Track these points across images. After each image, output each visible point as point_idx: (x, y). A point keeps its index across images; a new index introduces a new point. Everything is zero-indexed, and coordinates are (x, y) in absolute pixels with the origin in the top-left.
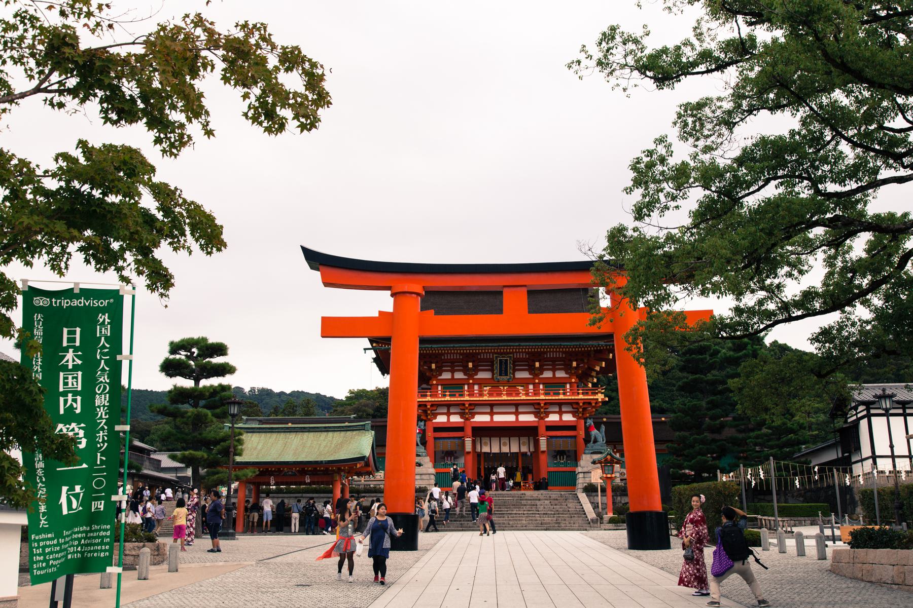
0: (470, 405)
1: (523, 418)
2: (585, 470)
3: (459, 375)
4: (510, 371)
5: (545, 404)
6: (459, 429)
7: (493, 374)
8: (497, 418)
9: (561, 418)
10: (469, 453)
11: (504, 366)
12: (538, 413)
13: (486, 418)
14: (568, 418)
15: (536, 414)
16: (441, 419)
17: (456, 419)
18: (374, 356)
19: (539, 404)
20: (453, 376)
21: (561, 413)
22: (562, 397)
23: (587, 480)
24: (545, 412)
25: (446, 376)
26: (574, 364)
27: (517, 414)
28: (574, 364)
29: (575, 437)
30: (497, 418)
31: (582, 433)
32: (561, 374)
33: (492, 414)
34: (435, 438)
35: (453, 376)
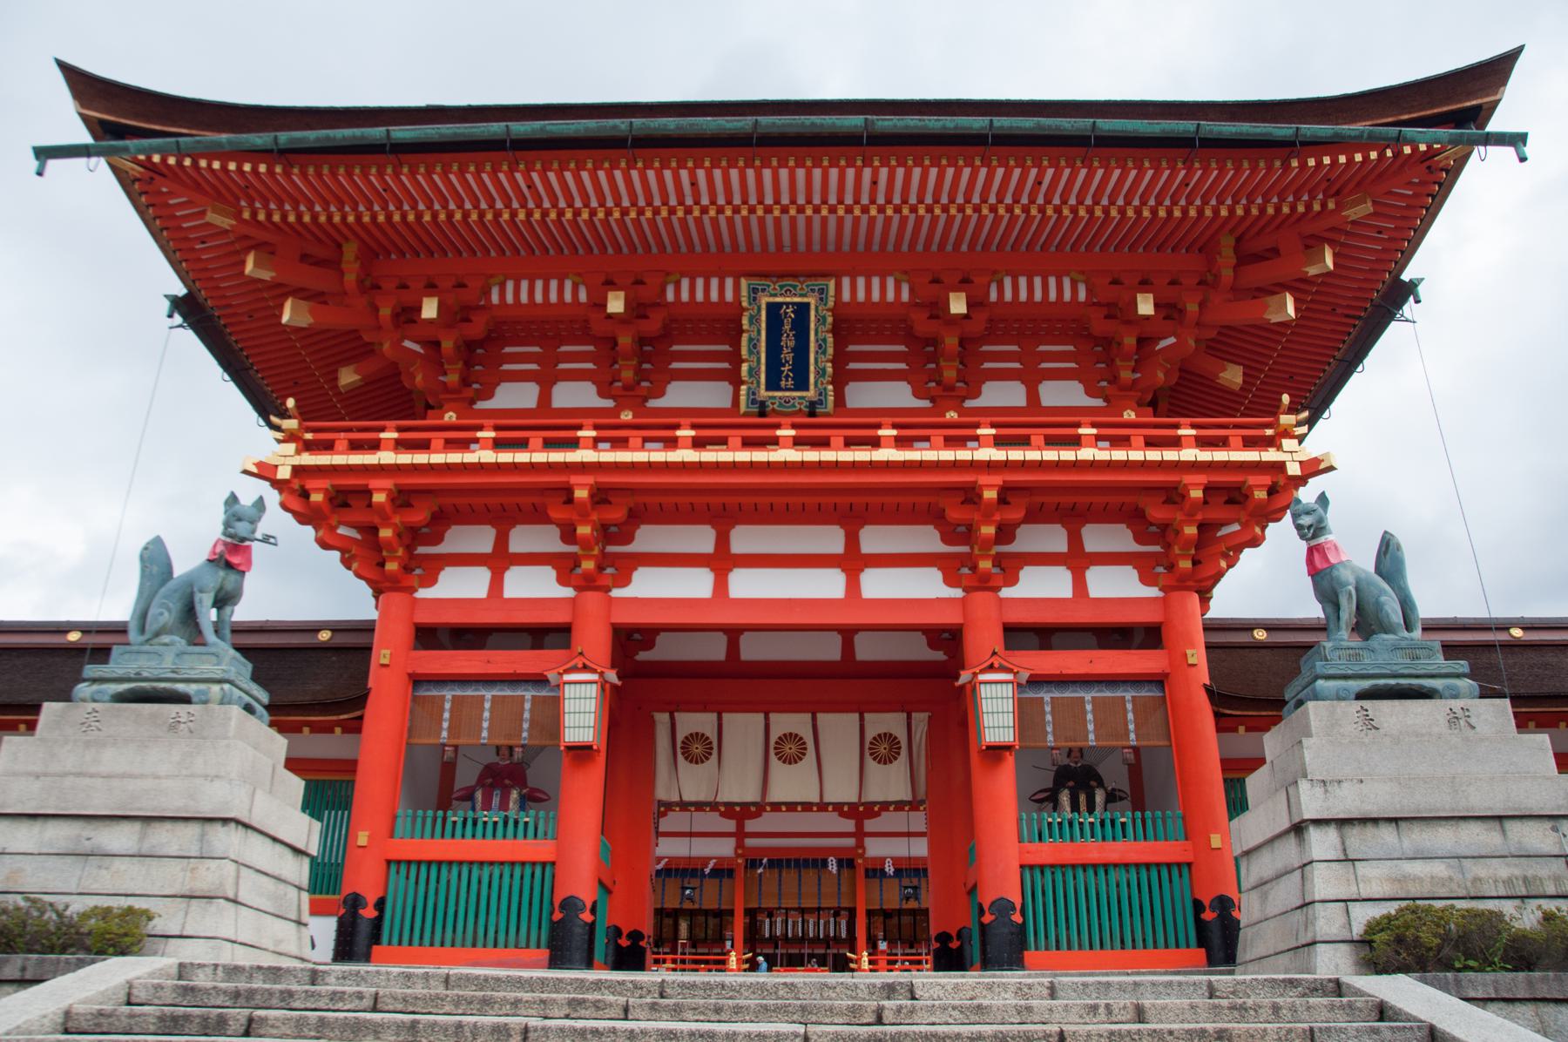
0: (601, 496)
1: (879, 585)
2: (1346, 802)
3: (574, 395)
4: (819, 361)
5: (1006, 493)
6: (546, 634)
7: (737, 382)
8: (747, 584)
9: (1080, 584)
10: (581, 752)
11: (788, 341)
12: (962, 559)
13: (695, 584)
14: (1116, 586)
15: (950, 568)
16: (461, 586)
17: (533, 586)
18: (180, 290)
19: (970, 495)
20: (545, 397)
21: (1077, 560)
22: (1086, 454)
23: (1375, 878)
24: (999, 560)
25: (516, 396)
26: (1146, 306)
27: (853, 562)
28: (1146, 306)
29: (1158, 680)
30: (747, 584)
31: (1197, 656)
32: (1061, 394)
33: (722, 562)
34: (417, 681)
35: (545, 397)
